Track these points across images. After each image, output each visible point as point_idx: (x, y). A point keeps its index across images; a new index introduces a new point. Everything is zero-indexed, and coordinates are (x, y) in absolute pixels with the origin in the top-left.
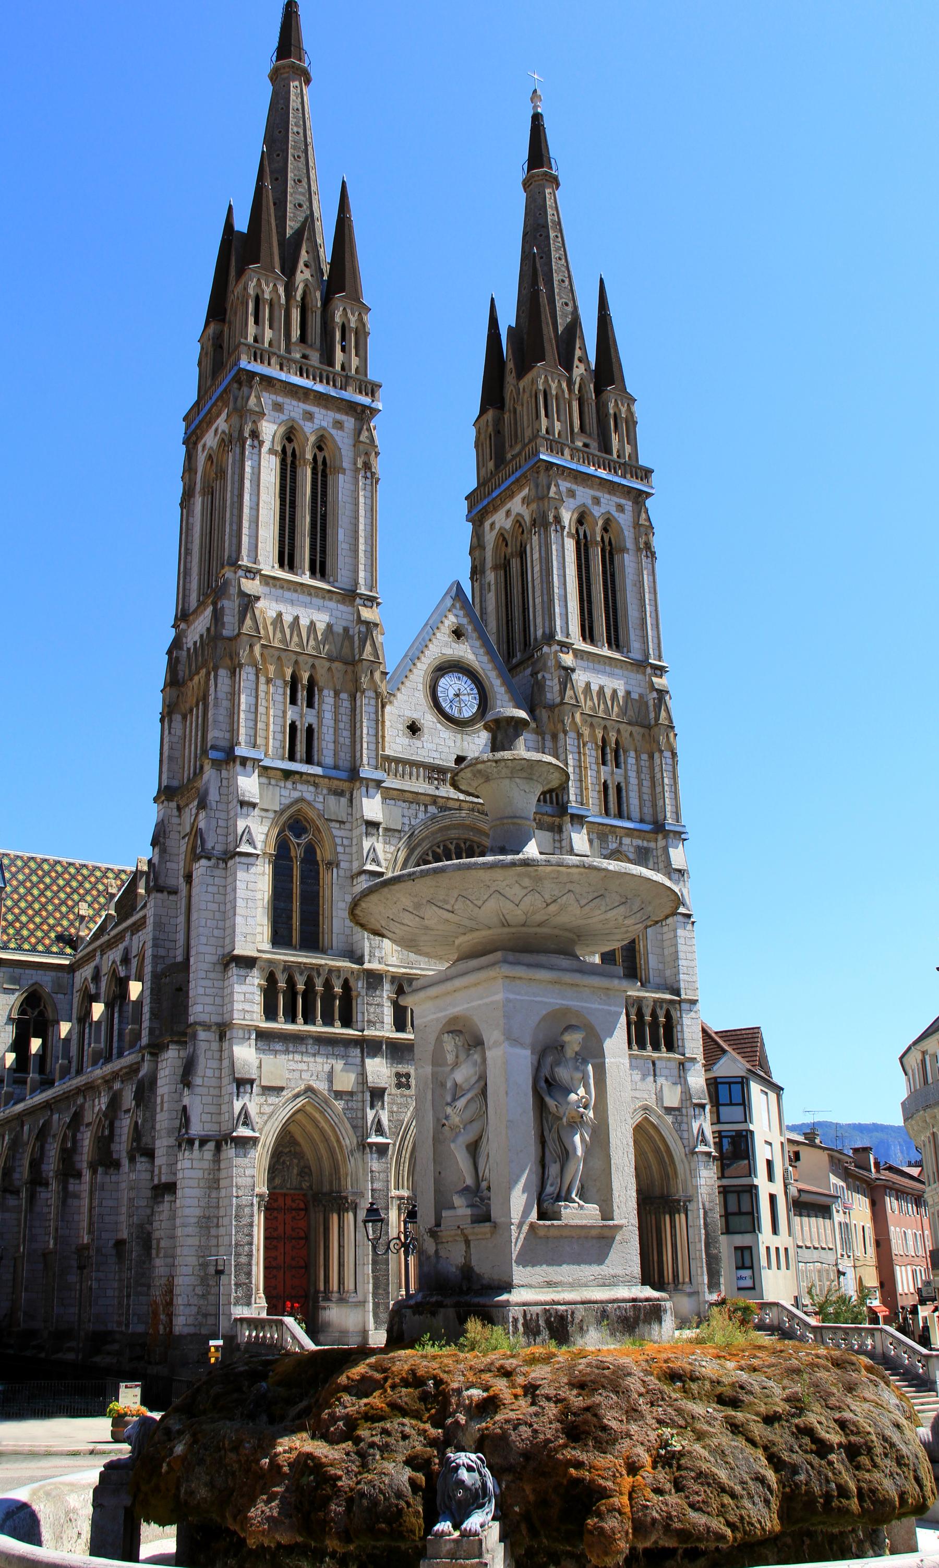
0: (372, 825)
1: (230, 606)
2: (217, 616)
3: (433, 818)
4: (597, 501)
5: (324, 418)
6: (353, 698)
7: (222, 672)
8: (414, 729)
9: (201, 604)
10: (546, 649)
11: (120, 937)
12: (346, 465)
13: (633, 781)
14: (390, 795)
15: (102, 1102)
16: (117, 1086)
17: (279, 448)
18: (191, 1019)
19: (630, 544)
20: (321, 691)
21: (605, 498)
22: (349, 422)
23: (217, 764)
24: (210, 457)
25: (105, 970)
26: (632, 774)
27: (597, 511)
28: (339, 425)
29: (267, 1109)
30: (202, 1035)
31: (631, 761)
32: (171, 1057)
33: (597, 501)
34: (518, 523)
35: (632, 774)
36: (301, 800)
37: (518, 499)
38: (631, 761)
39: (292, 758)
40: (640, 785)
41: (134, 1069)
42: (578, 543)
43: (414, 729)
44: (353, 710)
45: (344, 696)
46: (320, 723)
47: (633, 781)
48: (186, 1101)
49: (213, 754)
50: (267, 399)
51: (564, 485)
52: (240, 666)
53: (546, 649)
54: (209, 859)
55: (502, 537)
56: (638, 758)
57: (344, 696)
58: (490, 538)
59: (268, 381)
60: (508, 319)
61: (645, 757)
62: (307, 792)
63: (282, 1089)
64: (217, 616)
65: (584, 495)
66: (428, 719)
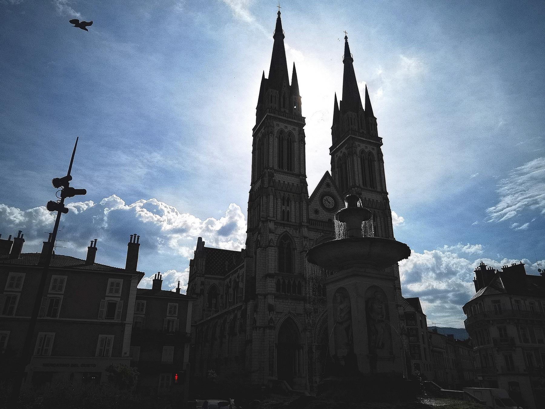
0: (305, 238)
1: (266, 179)
2: (263, 182)
3: (323, 236)
4: (366, 147)
5: (290, 128)
6: (300, 203)
7: (264, 197)
8: (316, 212)
9: (258, 179)
10: (353, 189)
11: (237, 271)
12: (296, 140)
13: (379, 225)
14: (309, 229)
15: (232, 317)
16: (236, 312)
17: (278, 136)
18: (257, 293)
19: (376, 159)
20: (291, 201)
21: (369, 146)
22: (297, 129)
23: (263, 222)
24: (259, 140)
25: (232, 280)
26: (379, 224)
27: (366, 150)
28: (294, 129)
29: (278, 319)
30: (259, 297)
31: (378, 220)
32: (250, 304)
33: (366, 147)
34: (344, 154)
35: (379, 224)
36: (286, 231)
37: (344, 148)
38: (378, 220)
39: (283, 220)
40: (381, 226)
41: (241, 307)
42: (361, 159)
43: (316, 212)
44: (300, 207)
45: (297, 203)
46: (291, 211)
47: (379, 225)
48: (255, 316)
49: (262, 219)
50: (275, 123)
51: (357, 143)
52: (269, 195)
53: (353, 189)
54: (261, 247)
55: (340, 159)
56: (380, 219)
57: (297, 203)
58: (336, 159)
59: (275, 118)
60: (340, 98)
61: (382, 218)
62: (288, 229)
63: (282, 313)
64: (263, 182)
65: (363, 146)
66: (320, 209)
